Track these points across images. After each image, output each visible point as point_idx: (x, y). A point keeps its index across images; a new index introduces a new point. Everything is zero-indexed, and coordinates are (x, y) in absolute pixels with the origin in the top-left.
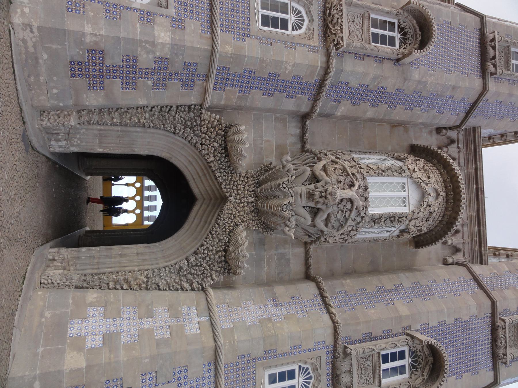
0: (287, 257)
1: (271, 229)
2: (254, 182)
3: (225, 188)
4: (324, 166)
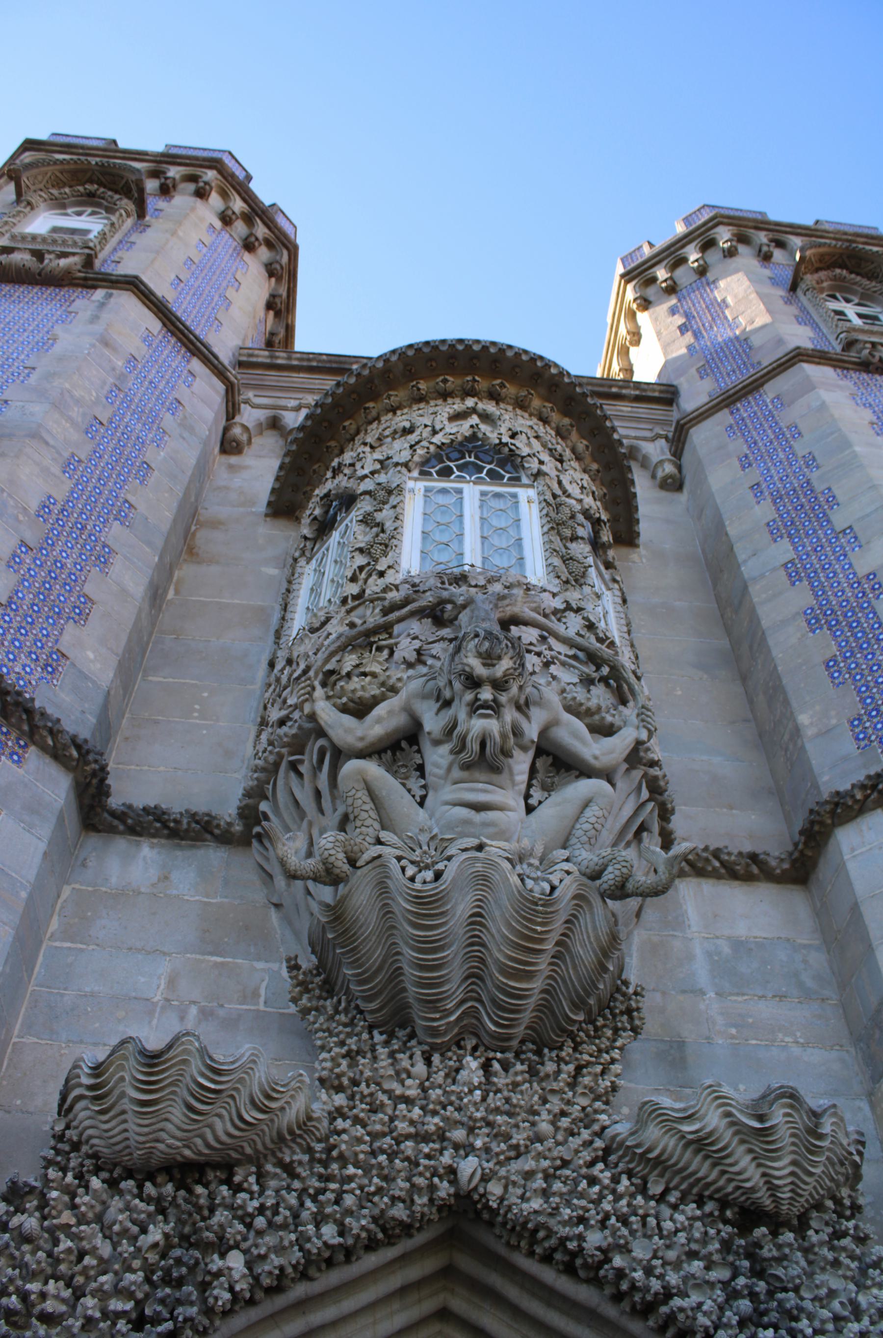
0: (727, 950)
1: (618, 990)
2: (382, 1052)
3: (410, 1203)
4: (344, 709)
